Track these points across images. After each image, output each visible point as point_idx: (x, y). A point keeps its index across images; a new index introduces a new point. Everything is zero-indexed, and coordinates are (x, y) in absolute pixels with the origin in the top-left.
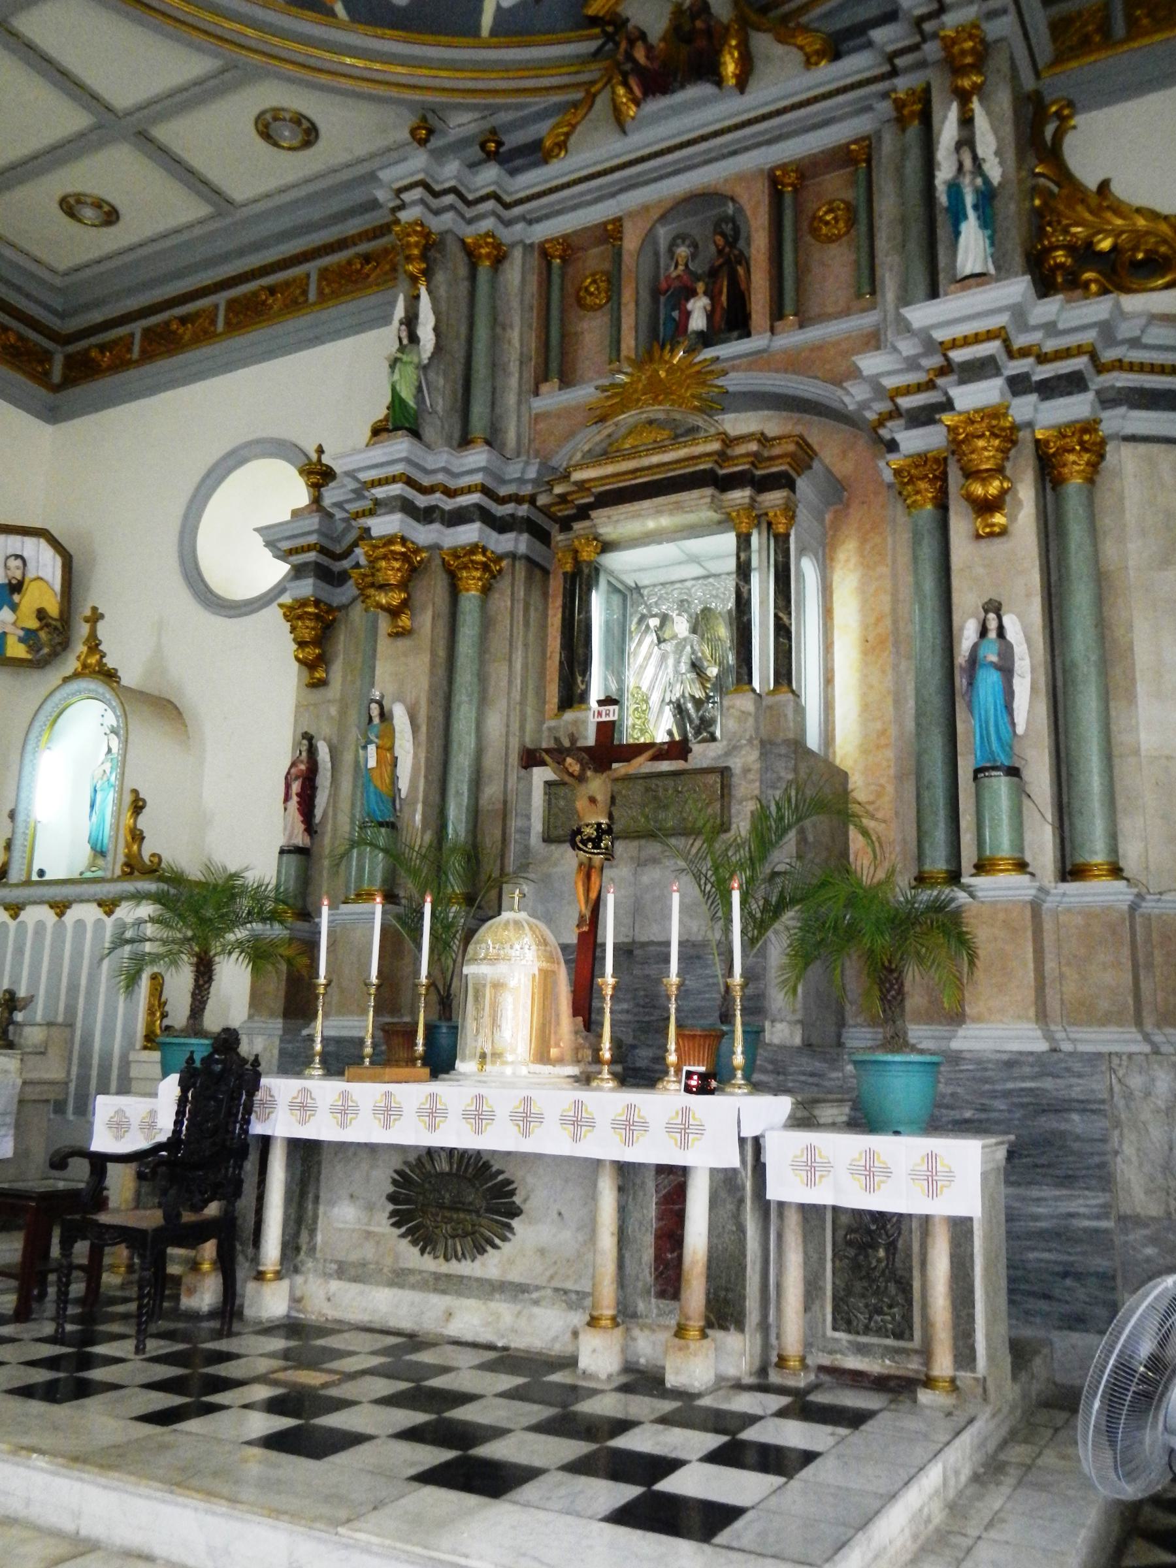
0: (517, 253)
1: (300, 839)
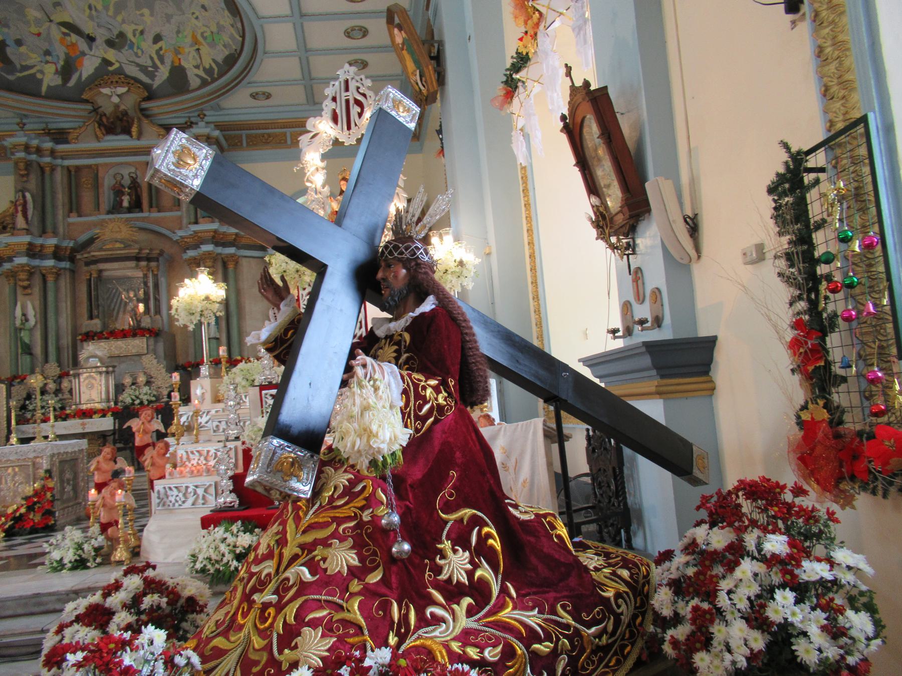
0: (59, 169)
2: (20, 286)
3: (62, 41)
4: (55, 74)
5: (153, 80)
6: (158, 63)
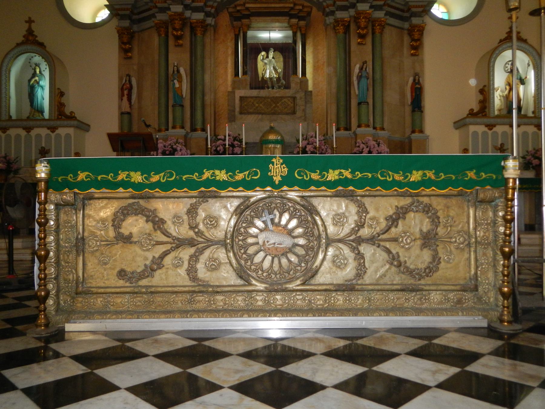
1: (128, 110)
2: (173, 35)
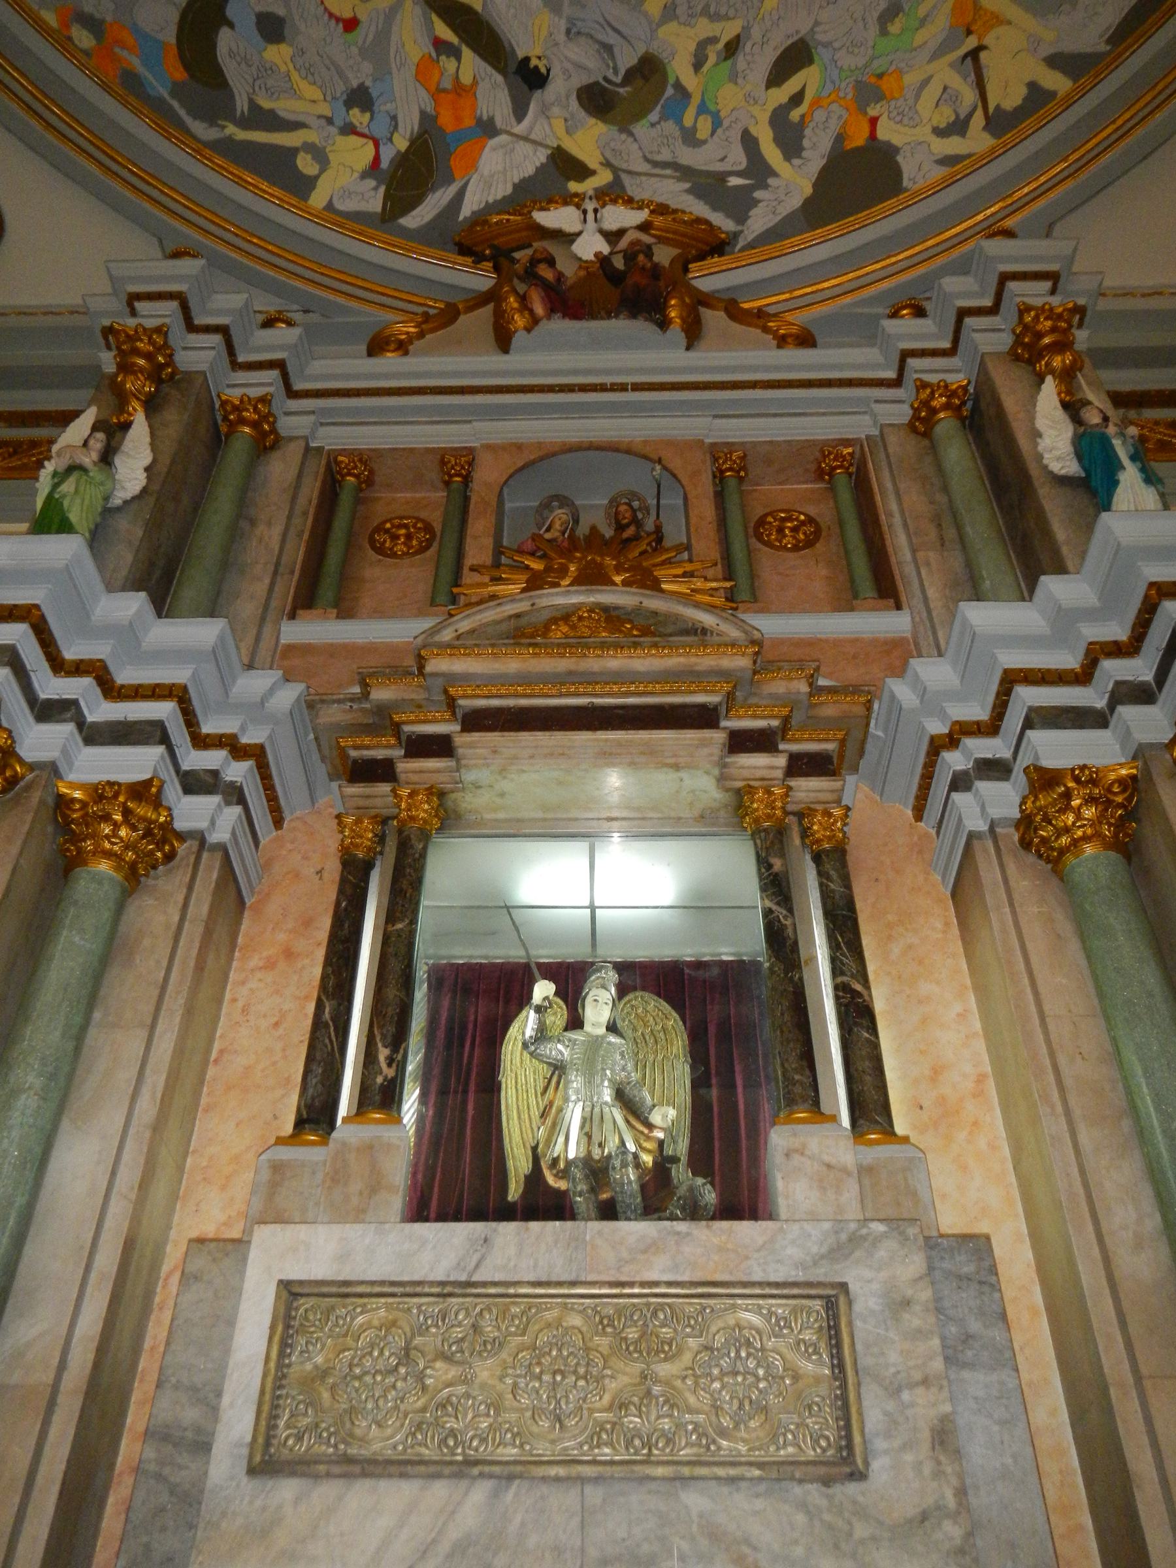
3: (422, 73)
4: (364, 175)
5: (741, 219)
6: (772, 153)
